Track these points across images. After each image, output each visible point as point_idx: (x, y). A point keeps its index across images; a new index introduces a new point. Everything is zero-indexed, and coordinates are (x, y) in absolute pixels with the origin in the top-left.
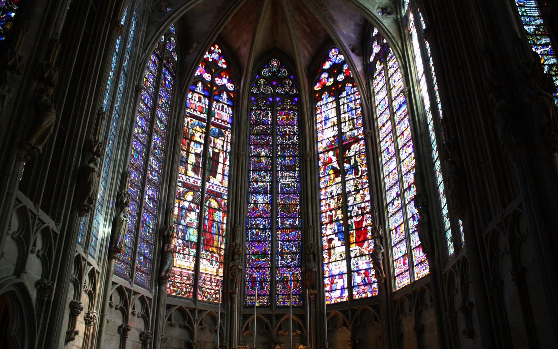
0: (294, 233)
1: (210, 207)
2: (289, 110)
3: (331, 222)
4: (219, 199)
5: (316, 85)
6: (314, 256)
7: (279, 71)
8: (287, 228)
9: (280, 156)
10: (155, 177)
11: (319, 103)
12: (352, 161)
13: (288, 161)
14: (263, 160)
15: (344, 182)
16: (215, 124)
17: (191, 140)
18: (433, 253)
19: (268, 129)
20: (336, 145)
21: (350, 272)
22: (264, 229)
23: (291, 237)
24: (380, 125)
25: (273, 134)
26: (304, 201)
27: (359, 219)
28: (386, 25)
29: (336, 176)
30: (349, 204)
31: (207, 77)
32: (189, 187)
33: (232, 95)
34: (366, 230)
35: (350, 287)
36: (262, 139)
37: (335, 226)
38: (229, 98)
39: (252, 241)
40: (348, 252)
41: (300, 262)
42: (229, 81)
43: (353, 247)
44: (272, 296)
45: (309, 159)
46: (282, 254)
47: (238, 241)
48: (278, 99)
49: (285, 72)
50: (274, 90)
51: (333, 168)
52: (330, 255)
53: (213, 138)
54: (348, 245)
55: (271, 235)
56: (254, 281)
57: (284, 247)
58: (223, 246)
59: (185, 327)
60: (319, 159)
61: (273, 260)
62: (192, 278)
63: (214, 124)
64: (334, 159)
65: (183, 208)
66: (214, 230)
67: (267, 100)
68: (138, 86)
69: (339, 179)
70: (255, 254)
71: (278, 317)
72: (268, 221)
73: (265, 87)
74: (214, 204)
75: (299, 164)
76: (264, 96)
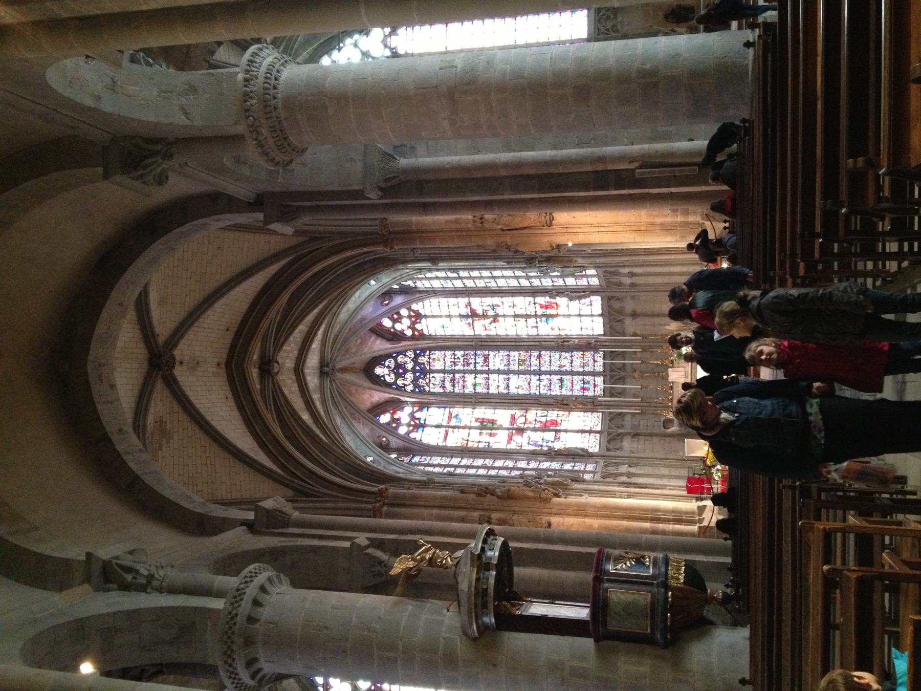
0: (543, 357)
1: (525, 423)
2: (429, 358)
3: (537, 327)
4: (516, 417)
5: (405, 334)
6: (564, 342)
7: (389, 367)
8: (540, 363)
9: (475, 367)
10: (510, 464)
11: (426, 332)
12: (486, 308)
13: (480, 360)
14: (478, 380)
15: (504, 316)
16: (449, 421)
17: (468, 440)
18: (583, 267)
19: (448, 377)
20: (470, 320)
21: (580, 315)
22: (539, 380)
23: (547, 359)
24: (463, 286)
25: (453, 372)
26: (517, 348)
27: (538, 306)
28: (388, 280)
29: (498, 321)
30: (524, 313)
31: (402, 430)
32: (510, 439)
33: (416, 409)
34: (548, 302)
35: (592, 316)
36: (458, 382)
37: (540, 324)
38: (421, 409)
39: (550, 390)
40: (564, 316)
41: (568, 352)
42: (402, 409)
43: (561, 311)
44: (594, 374)
45: (480, 343)
46: (561, 366)
47: (552, 401)
48: (418, 368)
49: (390, 362)
50: (409, 371)
51: (490, 324)
52: (564, 330)
53: (462, 424)
54: (557, 316)
55: (545, 374)
56: (584, 389)
57: (556, 364)
58: (556, 412)
59: (622, 438)
60: (480, 335)
61: (567, 373)
62: (584, 435)
63: (449, 421)
64: (482, 322)
65: (529, 444)
66: (543, 419)
67: (419, 378)
68: (448, 475)
69: (500, 319)
70: (561, 387)
71: (612, 371)
72: (533, 377)
73: (406, 379)
74: (522, 419)
75: (482, 350)
76: (415, 381)
